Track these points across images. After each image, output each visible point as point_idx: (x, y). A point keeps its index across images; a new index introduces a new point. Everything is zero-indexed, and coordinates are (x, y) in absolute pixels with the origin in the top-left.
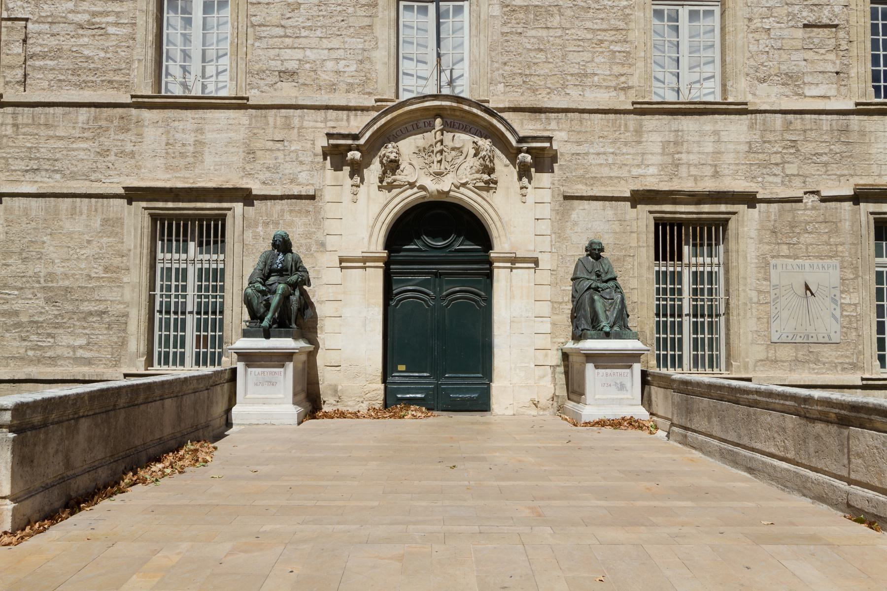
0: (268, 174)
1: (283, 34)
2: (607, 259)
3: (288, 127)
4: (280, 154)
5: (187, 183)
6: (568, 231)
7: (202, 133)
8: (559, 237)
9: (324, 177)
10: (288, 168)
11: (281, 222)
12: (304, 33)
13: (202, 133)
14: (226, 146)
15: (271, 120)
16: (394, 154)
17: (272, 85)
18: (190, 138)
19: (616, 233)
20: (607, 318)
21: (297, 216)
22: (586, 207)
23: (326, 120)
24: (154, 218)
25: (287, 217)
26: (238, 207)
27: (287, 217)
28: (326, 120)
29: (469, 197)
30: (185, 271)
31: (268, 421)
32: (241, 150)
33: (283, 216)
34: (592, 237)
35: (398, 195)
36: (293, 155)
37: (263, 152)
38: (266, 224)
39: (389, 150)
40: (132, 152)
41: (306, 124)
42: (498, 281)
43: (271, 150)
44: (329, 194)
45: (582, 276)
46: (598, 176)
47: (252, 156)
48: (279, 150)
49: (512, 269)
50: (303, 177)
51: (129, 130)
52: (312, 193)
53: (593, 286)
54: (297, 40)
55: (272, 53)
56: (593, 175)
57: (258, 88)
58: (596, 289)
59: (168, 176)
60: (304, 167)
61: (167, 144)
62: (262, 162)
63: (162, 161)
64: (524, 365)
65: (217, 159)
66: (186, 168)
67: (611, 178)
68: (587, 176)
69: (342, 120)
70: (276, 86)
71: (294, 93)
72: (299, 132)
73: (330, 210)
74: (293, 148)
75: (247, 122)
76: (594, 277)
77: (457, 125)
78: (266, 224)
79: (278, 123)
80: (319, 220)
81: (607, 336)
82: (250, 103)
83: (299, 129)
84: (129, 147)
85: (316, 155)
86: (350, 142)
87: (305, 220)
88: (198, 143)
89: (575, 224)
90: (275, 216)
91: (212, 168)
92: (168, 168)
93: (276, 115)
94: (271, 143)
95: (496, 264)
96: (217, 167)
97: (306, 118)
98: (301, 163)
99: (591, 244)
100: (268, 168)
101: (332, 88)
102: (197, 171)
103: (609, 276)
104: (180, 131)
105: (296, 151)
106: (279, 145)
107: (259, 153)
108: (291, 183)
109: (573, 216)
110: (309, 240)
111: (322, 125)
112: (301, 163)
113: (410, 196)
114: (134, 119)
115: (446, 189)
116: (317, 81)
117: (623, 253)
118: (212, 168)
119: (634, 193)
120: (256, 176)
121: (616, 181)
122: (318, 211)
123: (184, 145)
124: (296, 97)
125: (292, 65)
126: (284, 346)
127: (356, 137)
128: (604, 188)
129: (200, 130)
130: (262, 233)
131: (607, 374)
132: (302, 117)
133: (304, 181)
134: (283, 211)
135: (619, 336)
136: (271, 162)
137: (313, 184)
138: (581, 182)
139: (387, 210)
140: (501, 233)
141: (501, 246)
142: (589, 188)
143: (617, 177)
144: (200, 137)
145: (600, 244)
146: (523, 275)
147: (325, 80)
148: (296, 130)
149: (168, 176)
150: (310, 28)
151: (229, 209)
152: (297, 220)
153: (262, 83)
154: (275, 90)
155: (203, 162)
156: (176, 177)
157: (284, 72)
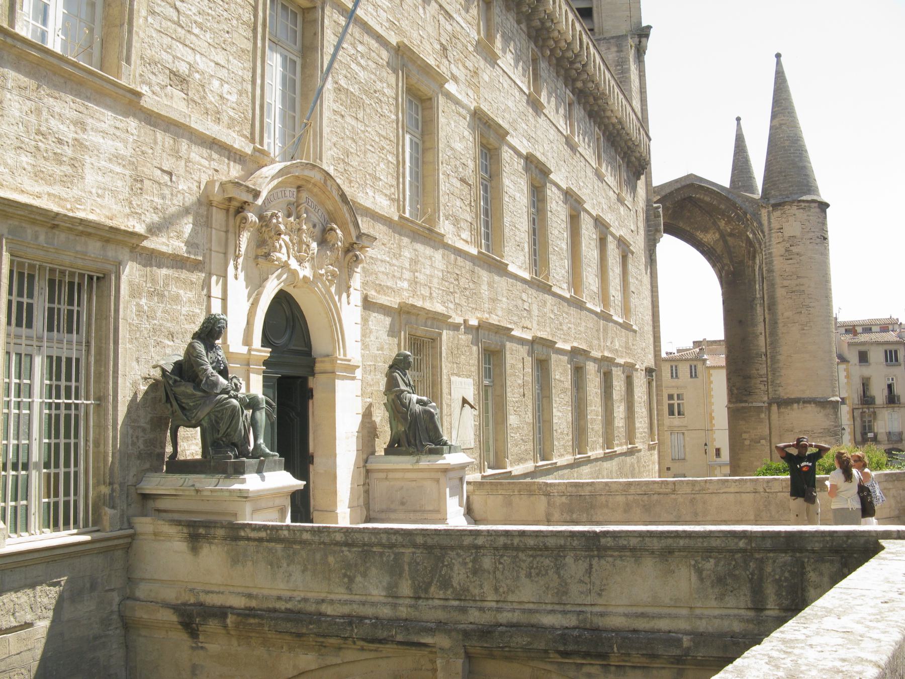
1: (176, 19)
4: (167, 192)
5: (63, 207)
12: (196, 31)
13: (84, 130)
21: (181, 288)
47: (139, 185)
54: (188, 36)
55: (166, 40)
63: (31, 160)
65: (100, 178)
71: (182, 106)
91: (94, 191)
92: (38, 175)
94: (159, 172)
96: (100, 192)
100: (155, 209)
123: (60, 142)
125: (183, 68)
130: (146, 308)
144: (81, 136)
149: (37, 189)
150: (200, 26)
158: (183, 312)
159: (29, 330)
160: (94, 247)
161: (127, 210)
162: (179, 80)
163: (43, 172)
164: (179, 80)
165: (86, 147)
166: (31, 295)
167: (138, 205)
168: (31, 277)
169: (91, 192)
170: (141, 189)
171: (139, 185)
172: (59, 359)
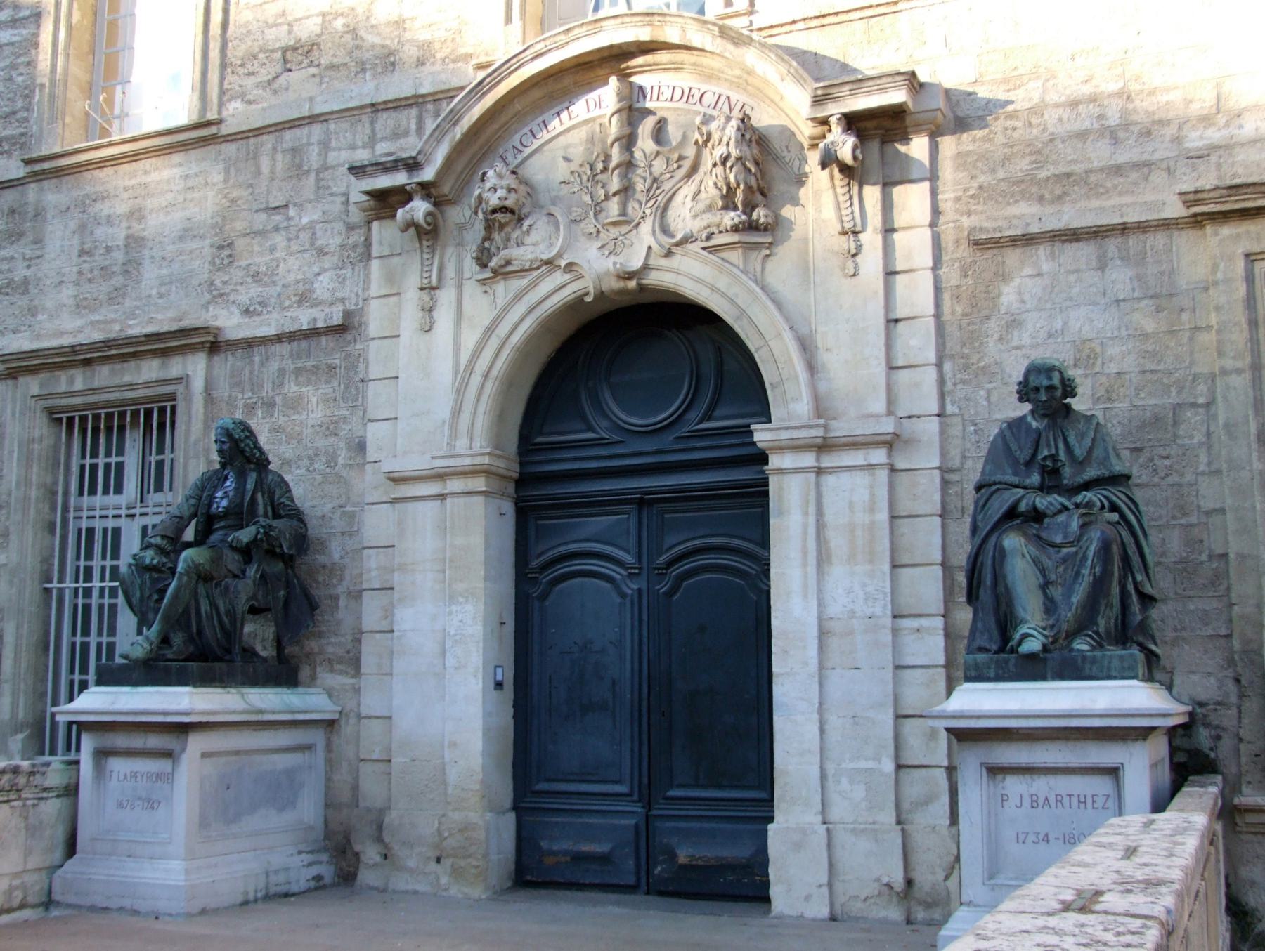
0: (255, 290)
2: (1089, 419)
4: (279, 239)
6: (992, 345)
7: (141, 218)
8: (966, 367)
9: (367, 276)
10: (293, 268)
11: (278, 400)
14: (181, 238)
15: (265, 163)
16: (501, 193)
17: (269, 82)
19: (1145, 336)
20: (1050, 607)
22: (1046, 267)
23: (372, 141)
24: (55, 416)
25: (292, 388)
27: (292, 388)
28: (372, 141)
29: (691, 277)
30: (117, 532)
31: (127, 903)
32: (208, 242)
33: (281, 384)
34: (1058, 353)
35: (518, 297)
36: (305, 237)
37: (248, 239)
39: (488, 185)
40: (26, 281)
41: (333, 157)
42: (781, 513)
43: (261, 233)
44: (375, 321)
45: (998, 478)
46: (1077, 168)
47: (227, 252)
48: (277, 229)
49: (819, 471)
50: (324, 286)
51: (21, 235)
52: (337, 320)
53: (1023, 507)
56: (1062, 169)
57: (242, 96)
58: (1037, 516)
59: (79, 322)
60: (328, 262)
61: (82, 253)
62: (243, 263)
64: (863, 764)
65: (165, 272)
66: (110, 300)
67: (1118, 170)
68: (1043, 174)
69: (406, 133)
70: (276, 86)
72: (318, 180)
73: (376, 358)
74: (305, 220)
75: (221, 177)
76: (1035, 479)
77: (668, 94)
79: (279, 166)
80: (353, 384)
81: (1033, 668)
82: (225, 130)
83: (318, 171)
84: (21, 272)
85: (350, 228)
86: (400, 179)
87: (325, 389)
89: (1014, 323)
90: (268, 386)
92: (80, 306)
93: (274, 149)
94: (263, 216)
95: (775, 461)
96: (163, 290)
97: (333, 144)
98: (321, 252)
99: (1034, 369)
100: (256, 276)
102: (129, 303)
103: (1091, 473)
104: (103, 221)
105: (311, 226)
106: (278, 218)
107: (240, 244)
108: (300, 303)
109: (1004, 300)
110: (332, 440)
112: (321, 252)
114: (30, 209)
115: (636, 263)
116: (357, 53)
117: (1174, 398)
118: (154, 292)
119: (1191, 198)
120: (232, 298)
121: (1134, 176)
122: (353, 363)
124: (311, 99)
126: (173, 707)
127: (413, 165)
128: (1095, 203)
131: (1034, 803)
132: (325, 146)
133: (327, 295)
134: (282, 372)
135: (1073, 670)
136: (261, 261)
137: (343, 300)
138: (1024, 195)
139: (494, 343)
140: (785, 373)
141: (790, 405)
142: (1050, 209)
143: (1137, 166)
145: (1048, 370)
146: (854, 493)
147: (373, 46)
148: (312, 177)
149: (79, 322)
151: (178, 380)
152: (308, 391)
153: (250, 82)
154: (275, 92)
155: (139, 282)
156: (92, 323)
157: (295, 49)
158: (311, 422)
159: (117, 497)
160: (150, 370)
161: (208, 296)
163: (86, 299)
165: (143, 239)
166: (121, 452)
167: (225, 283)
168: (122, 429)
169: (150, 296)
170: (230, 256)
171: (227, 252)
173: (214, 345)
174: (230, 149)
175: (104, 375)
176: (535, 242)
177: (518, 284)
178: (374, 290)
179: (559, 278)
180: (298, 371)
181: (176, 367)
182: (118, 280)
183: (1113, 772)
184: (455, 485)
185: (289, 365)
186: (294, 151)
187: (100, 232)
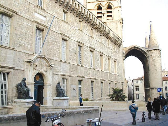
3: (20, 56)
18: (4, 55)
26: (12, 70)
38: (16, 75)
71: (21, 49)
78: (16, 75)
88: (5, 56)
101: (27, 50)
107: (16, 60)
111: (25, 56)
113: (37, 72)
125: (21, 44)
127: (32, 60)
129: (6, 54)
160: (7, 70)
162: (20, 45)
164: (20, 45)
172: (3, 84)
173: (14, 69)
174: (15, 51)
175: (3, 69)
176: (37, 68)
177: (36, 70)
178: (26, 68)
179: (38, 71)
180: (20, 73)
181: (10, 70)
182: (4, 60)
183: (68, 101)
184: (32, 84)
185: (19, 72)
186: (20, 54)
187: (2, 54)
